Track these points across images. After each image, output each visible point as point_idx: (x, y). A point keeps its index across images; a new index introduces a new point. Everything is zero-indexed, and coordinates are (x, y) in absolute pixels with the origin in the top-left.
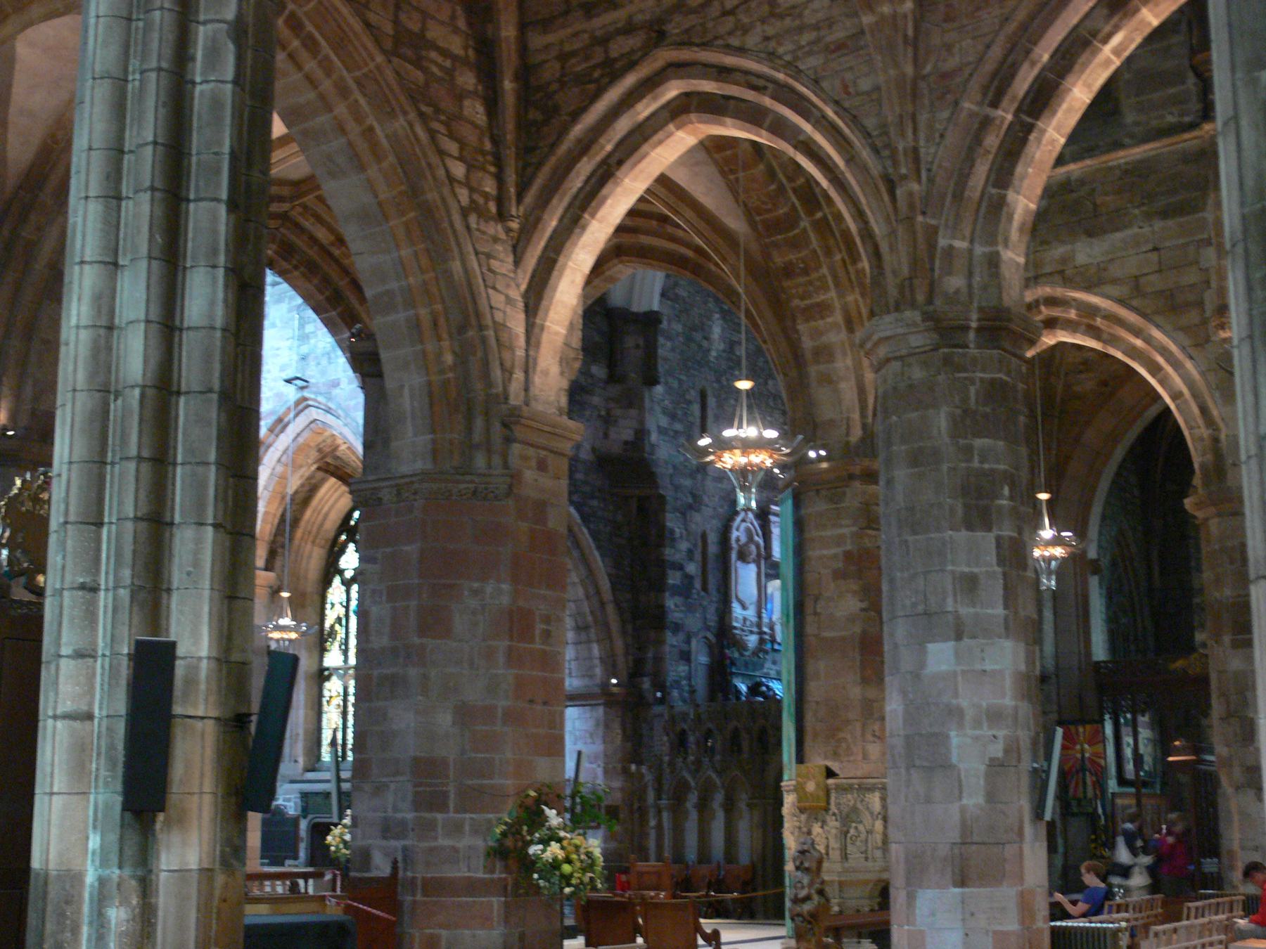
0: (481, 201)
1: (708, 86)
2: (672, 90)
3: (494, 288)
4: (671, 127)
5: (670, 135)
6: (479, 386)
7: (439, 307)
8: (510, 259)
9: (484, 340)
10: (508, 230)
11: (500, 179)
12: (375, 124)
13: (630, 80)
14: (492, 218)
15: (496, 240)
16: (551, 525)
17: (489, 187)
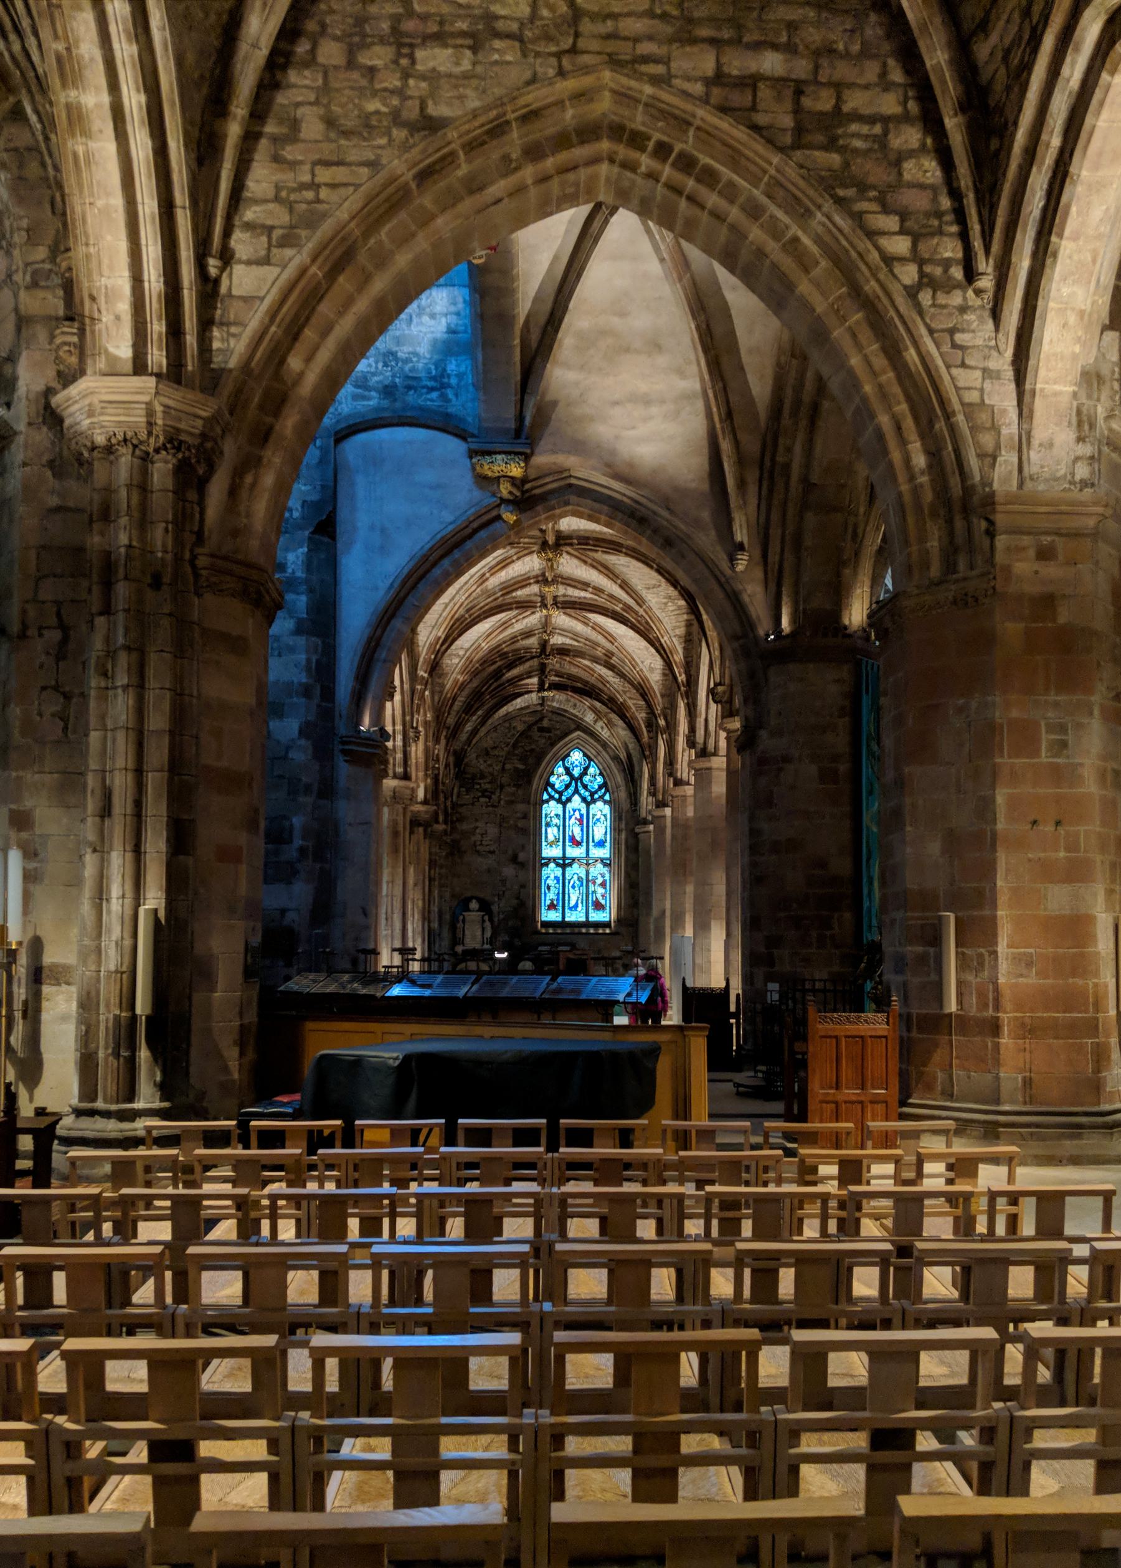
0: (938, 271)
3: (963, 365)
6: (955, 482)
7: (903, 408)
8: (990, 325)
9: (953, 429)
10: (978, 292)
11: (964, 236)
12: (800, 233)
14: (958, 286)
15: (963, 309)
16: (1062, 620)
17: (951, 249)
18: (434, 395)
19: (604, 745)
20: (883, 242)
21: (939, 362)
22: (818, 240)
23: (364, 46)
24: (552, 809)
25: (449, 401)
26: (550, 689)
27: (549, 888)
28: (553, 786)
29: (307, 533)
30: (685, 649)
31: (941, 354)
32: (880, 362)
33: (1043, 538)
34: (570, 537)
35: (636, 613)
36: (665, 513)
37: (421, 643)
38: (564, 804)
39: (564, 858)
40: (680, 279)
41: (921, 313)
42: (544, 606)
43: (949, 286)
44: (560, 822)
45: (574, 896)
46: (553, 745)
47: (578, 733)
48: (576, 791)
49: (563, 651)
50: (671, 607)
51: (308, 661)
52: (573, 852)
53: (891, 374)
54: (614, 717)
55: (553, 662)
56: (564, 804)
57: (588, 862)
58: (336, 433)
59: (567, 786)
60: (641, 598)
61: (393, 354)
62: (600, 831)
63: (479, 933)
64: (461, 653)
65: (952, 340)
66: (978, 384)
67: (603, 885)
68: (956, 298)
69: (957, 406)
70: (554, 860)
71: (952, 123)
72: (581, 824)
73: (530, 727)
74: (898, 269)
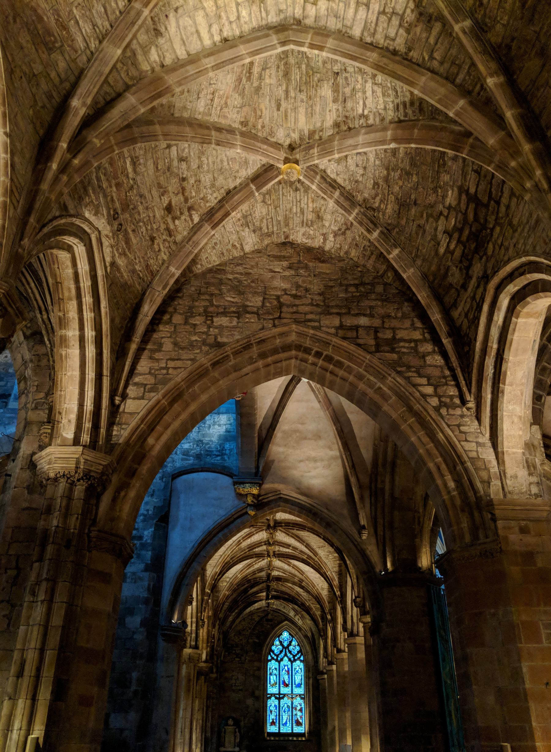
0: (448, 400)
1: (512, 288)
2: (504, 302)
3: (466, 440)
4: (514, 319)
5: (516, 323)
6: (471, 494)
7: (440, 459)
8: (476, 423)
9: (466, 470)
10: (468, 409)
11: (458, 386)
12: (382, 386)
13: (486, 308)
14: (458, 407)
15: (462, 416)
17: (453, 391)
18: (219, 458)
19: (300, 629)
20: (420, 388)
21: (455, 439)
22: (390, 388)
23: (192, 316)
24: (272, 665)
25: (225, 460)
26: (271, 599)
27: (271, 711)
28: (273, 652)
29: (155, 521)
30: (339, 578)
31: (455, 436)
32: (425, 439)
33: (521, 522)
35: (314, 560)
36: (325, 511)
37: (208, 575)
38: (279, 662)
39: (279, 694)
40: (328, 409)
41: (442, 417)
42: (269, 556)
43: (454, 407)
44: (277, 673)
45: (285, 717)
46: (273, 628)
47: (286, 622)
48: (286, 655)
49: (278, 579)
50: (331, 557)
51: (149, 585)
52: (284, 690)
53: (432, 445)
54: (304, 613)
55: (274, 585)
56: (279, 662)
57: (292, 696)
58: (173, 475)
59: (281, 652)
60: (316, 552)
61: (201, 441)
62: (299, 677)
64: (228, 580)
65: (459, 429)
66: (475, 449)
67: (301, 710)
68: (458, 412)
69: (466, 459)
71: (446, 341)
72: (288, 674)
73: (262, 619)
74: (429, 400)
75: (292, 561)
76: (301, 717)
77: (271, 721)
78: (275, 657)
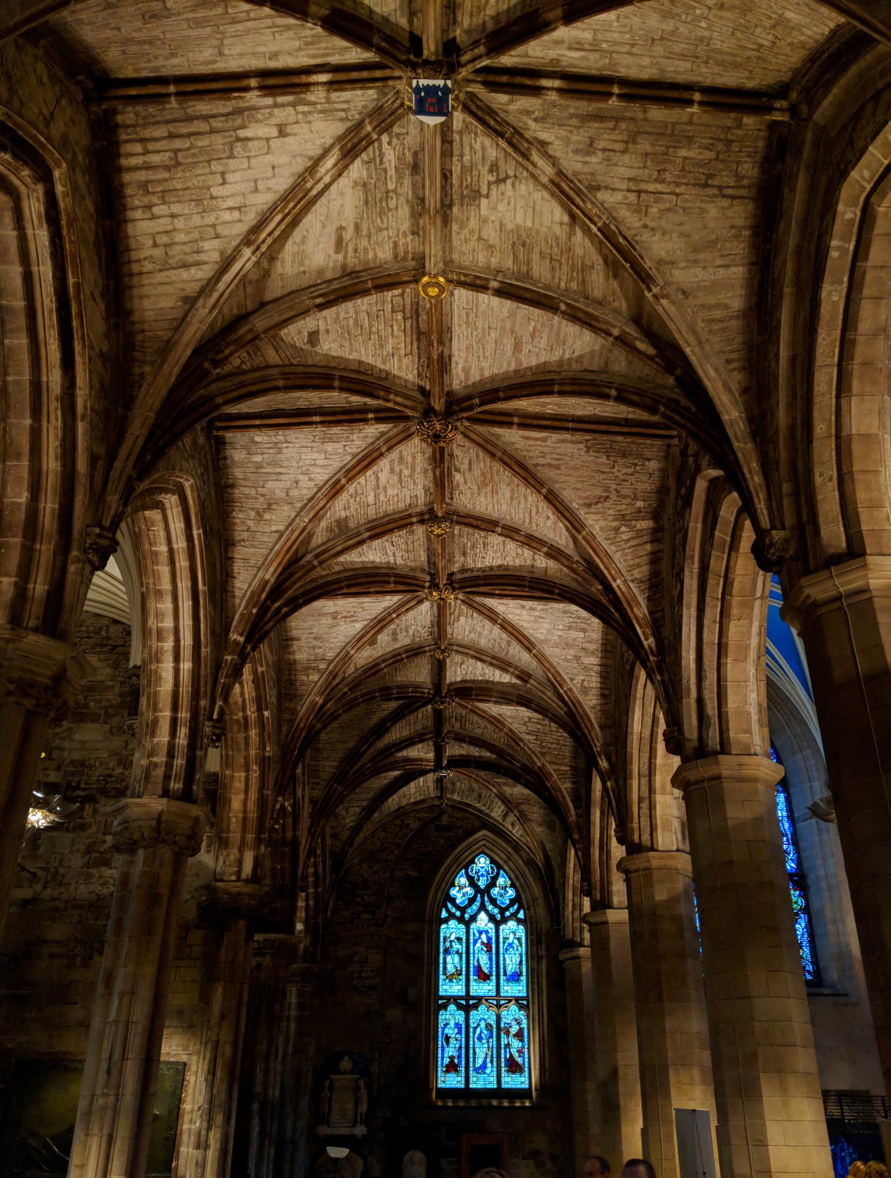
19: (517, 848)
24: (451, 930)
26: (448, 767)
27: (447, 1039)
28: (453, 900)
30: (649, 599)
34: (469, 397)
37: (238, 593)
38: (467, 924)
39: (468, 997)
42: (434, 586)
45: (481, 1052)
46: (453, 847)
47: (484, 832)
48: (483, 907)
50: (625, 533)
52: (480, 989)
55: (453, 708)
56: (467, 924)
57: (498, 1002)
59: (472, 901)
60: (578, 519)
62: (512, 960)
63: (350, 1106)
64: (322, 666)
67: (519, 1035)
70: (454, 999)
72: (489, 950)
75: (500, 606)
76: (520, 1052)
77: (447, 1061)
78: (458, 914)
